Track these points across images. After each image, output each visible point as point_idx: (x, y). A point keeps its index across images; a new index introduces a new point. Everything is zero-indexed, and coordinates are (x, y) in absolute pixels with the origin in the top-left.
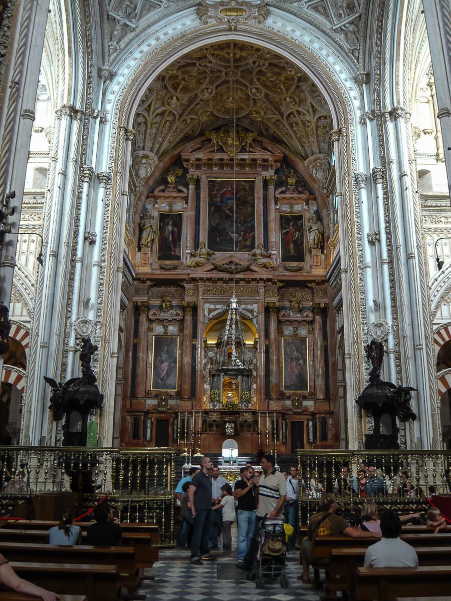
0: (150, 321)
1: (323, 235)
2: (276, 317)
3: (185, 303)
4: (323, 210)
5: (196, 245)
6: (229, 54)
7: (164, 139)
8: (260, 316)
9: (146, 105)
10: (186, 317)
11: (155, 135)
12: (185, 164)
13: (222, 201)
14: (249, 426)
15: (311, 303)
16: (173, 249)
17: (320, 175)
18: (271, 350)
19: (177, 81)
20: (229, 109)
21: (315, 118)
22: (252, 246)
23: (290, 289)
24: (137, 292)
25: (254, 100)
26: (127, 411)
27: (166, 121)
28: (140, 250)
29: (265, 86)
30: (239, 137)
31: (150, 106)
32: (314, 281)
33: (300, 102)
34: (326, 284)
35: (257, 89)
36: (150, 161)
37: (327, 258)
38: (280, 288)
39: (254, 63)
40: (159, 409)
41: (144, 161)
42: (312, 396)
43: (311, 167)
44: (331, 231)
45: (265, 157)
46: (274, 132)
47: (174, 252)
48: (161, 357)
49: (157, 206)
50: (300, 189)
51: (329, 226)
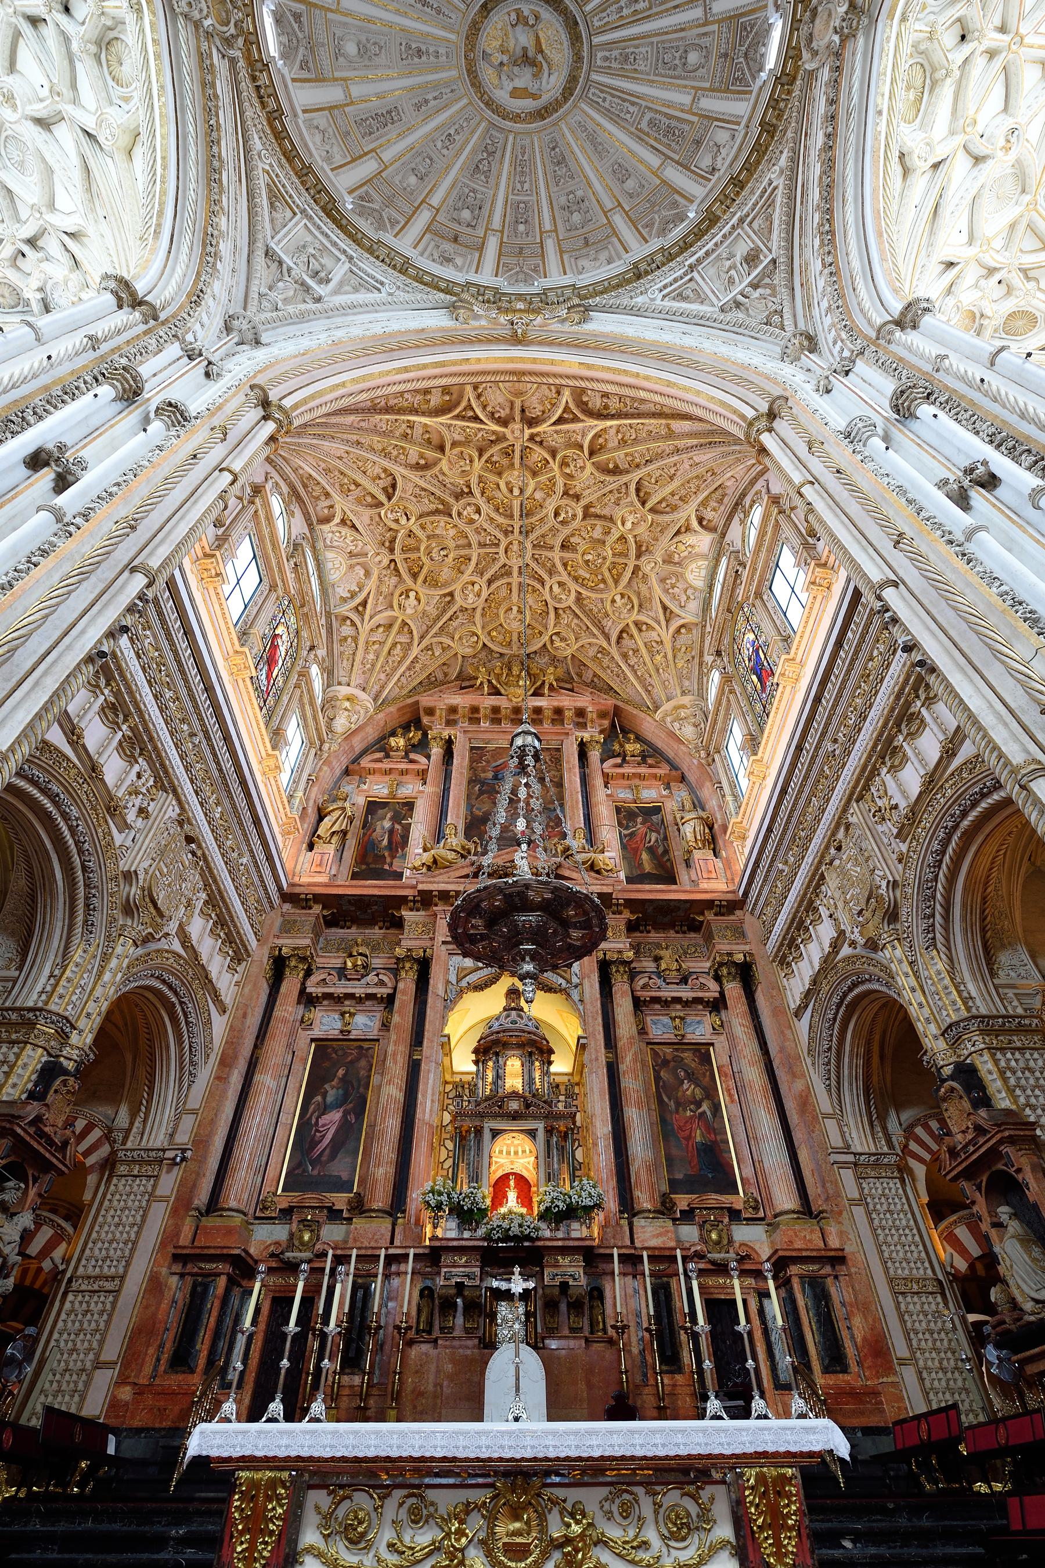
0: (308, 1000)
1: (711, 828)
2: (626, 987)
3: (399, 952)
4: (702, 786)
5: (439, 835)
6: (511, 491)
7: (389, 676)
8: (586, 982)
9: (359, 599)
10: (401, 985)
11: (373, 665)
12: (425, 720)
13: (496, 777)
14: (576, 1306)
15: (708, 964)
16: (388, 860)
17: (688, 732)
18: (622, 1067)
19: (413, 556)
20: (510, 633)
21: (672, 629)
22: (564, 836)
23: (653, 934)
24: (288, 927)
25: (556, 609)
26: (176, 1258)
27: (394, 645)
28: (311, 847)
29: (576, 579)
30: (529, 674)
31: (364, 603)
32: (709, 904)
33: (640, 606)
34: (738, 912)
35: (561, 584)
36: (358, 708)
37: (728, 864)
38: (632, 927)
39: (557, 514)
40: (288, 1254)
41: (347, 704)
42: (756, 1209)
43: (669, 719)
44: (731, 806)
45: (579, 704)
46: (595, 675)
47: (391, 865)
48: (324, 1095)
49: (365, 787)
50: (650, 761)
51: (720, 807)
